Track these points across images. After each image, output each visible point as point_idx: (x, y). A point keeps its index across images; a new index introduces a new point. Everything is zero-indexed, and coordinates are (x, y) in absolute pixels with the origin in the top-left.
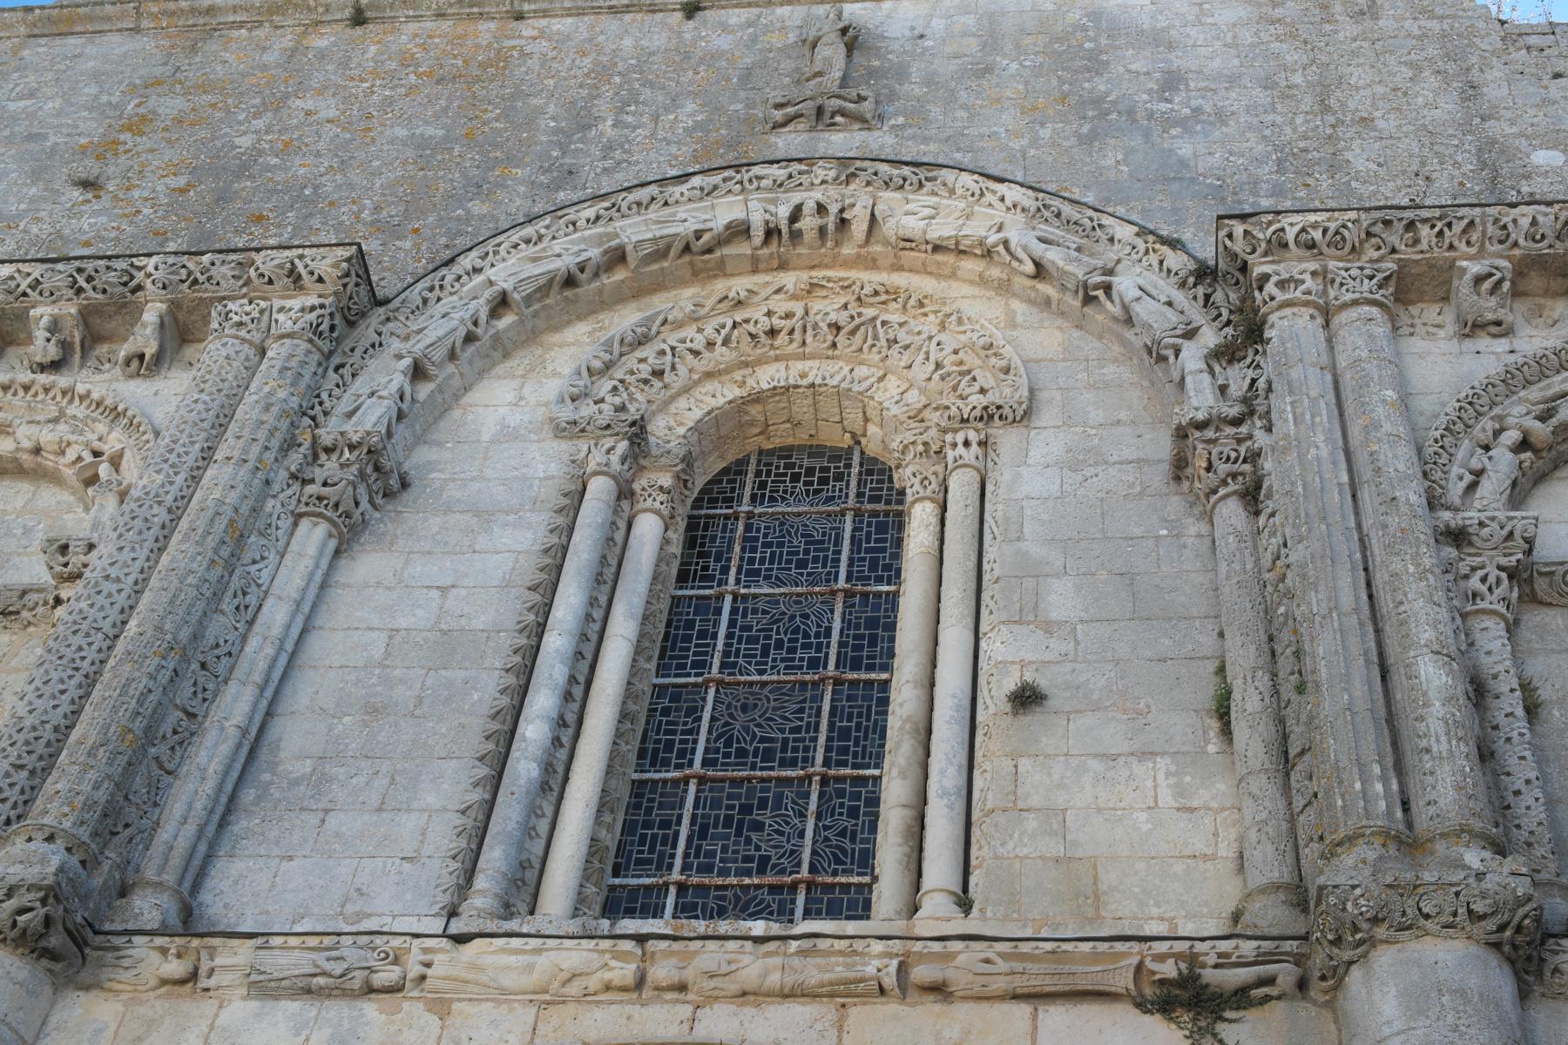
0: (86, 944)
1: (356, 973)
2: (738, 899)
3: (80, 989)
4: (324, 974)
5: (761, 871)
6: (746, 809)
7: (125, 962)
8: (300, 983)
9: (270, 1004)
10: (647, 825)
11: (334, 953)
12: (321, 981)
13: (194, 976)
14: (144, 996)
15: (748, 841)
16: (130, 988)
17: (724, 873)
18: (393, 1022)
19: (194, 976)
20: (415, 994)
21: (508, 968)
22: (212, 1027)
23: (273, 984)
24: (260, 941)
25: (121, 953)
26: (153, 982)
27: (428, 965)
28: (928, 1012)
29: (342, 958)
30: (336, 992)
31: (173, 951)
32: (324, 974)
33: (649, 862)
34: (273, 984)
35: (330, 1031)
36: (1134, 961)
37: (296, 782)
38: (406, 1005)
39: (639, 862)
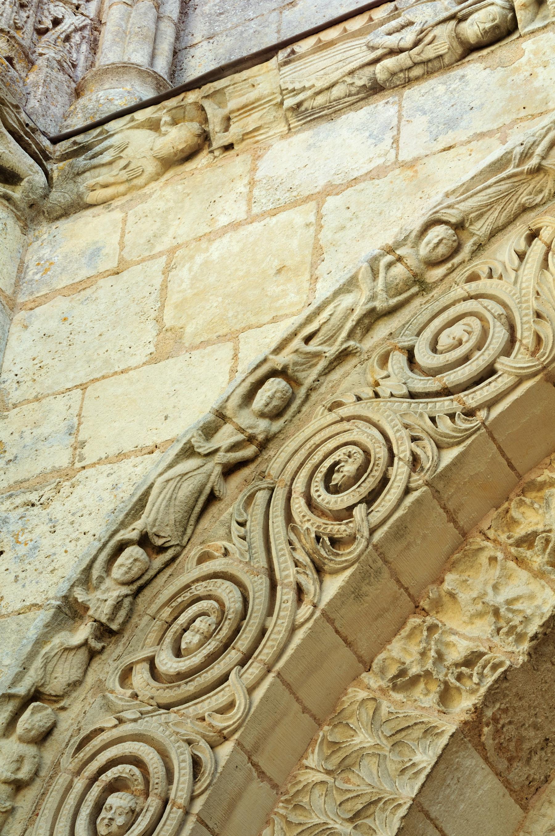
0: (47, 158)
1: (437, 31)
3: (57, 218)
4: (393, 52)
7: (106, 158)
8: (362, 79)
9: (324, 127)
11: (394, 24)
12: (390, 63)
14: (146, 190)
16: (122, 188)
18: (517, 69)
20: (538, 24)
22: (252, 183)
23: (320, 100)
24: (282, 55)
25: (97, 149)
26: (151, 167)
29: (411, 23)
30: (417, 72)
31: (166, 118)
32: (393, 52)
34: (320, 100)
35: (425, 119)
38: (528, 45)
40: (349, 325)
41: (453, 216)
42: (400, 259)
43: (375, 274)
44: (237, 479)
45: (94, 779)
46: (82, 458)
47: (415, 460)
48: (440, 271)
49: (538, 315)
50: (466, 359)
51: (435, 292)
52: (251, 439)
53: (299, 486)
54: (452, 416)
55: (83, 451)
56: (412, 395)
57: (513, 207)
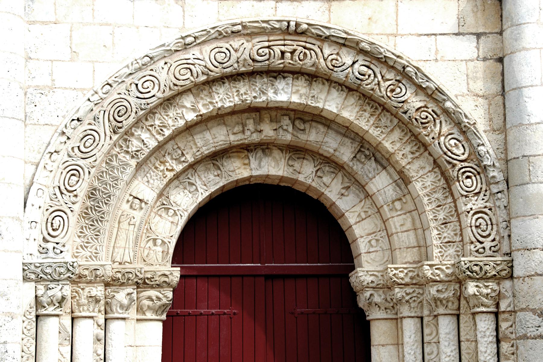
40: (125, 76)
41: (151, 56)
42: (138, 63)
43: (132, 64)
44: (97, 106)
45: (68, 172)
46: (54, 85)
47: (136, 112)
48: (145, 67)
49: (165, 86)
50: (149, 92)
51: (143, 71)
52: (101, 99)
53: (112, 113)
54: (145, 104)
55: (55, 82)
56: (137, 97)
57: (163, 56)
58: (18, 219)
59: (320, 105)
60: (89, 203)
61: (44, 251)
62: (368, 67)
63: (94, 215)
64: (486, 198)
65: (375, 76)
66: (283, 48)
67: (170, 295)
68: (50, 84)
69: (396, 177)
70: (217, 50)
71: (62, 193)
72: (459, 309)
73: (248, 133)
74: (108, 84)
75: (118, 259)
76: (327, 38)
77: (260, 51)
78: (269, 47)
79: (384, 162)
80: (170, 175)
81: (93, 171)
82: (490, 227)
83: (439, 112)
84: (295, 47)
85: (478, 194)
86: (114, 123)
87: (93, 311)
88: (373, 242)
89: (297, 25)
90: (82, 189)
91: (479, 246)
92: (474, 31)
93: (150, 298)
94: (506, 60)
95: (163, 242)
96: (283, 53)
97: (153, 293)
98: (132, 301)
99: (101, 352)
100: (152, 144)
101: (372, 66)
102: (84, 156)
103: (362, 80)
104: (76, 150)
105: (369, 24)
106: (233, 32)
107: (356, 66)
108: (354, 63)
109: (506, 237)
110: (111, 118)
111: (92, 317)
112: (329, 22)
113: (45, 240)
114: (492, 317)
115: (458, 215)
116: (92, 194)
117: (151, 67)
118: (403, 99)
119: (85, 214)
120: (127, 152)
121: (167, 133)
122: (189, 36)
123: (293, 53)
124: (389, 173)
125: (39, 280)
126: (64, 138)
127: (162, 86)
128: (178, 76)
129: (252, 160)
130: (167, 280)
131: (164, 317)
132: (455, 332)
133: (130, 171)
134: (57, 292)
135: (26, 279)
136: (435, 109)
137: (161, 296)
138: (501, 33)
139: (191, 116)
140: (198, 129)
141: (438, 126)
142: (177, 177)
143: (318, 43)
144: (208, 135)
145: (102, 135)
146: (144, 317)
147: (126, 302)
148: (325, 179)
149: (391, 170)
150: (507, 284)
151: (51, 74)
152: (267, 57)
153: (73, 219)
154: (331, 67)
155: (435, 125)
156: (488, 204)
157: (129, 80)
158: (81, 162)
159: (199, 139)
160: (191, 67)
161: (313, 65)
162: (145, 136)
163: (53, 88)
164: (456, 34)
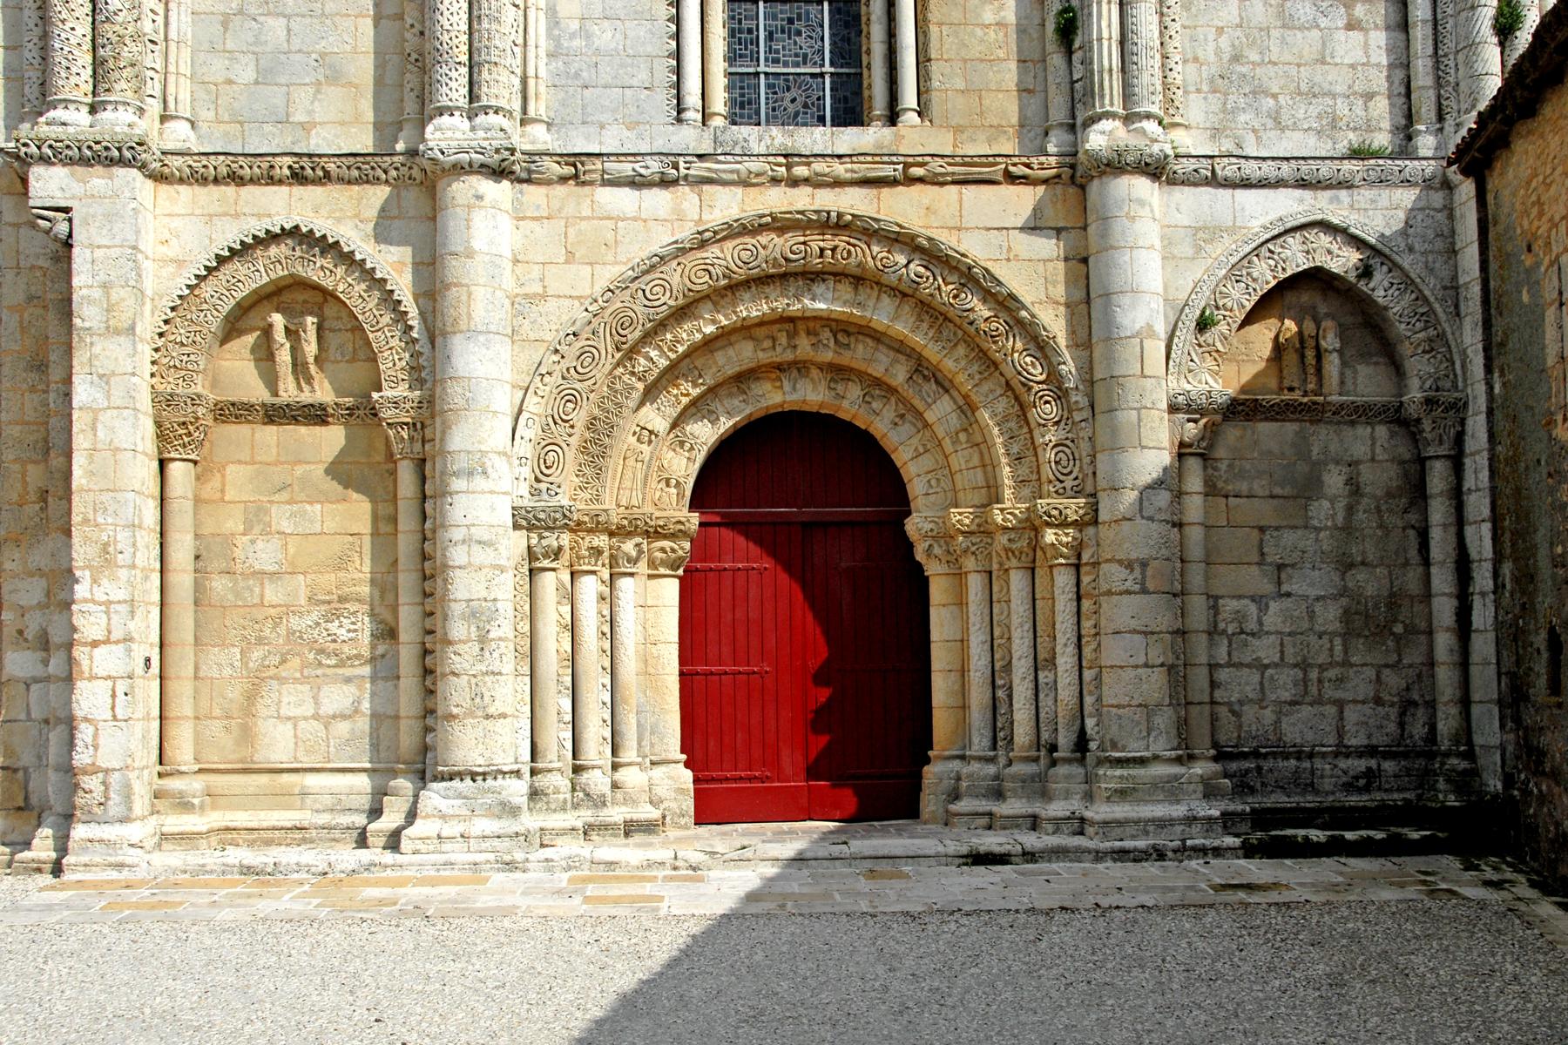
2: (795, 81)
5: (805, 63)
6: (791, 21)
10: (740, 31)
13: (576, 176)
15: (795, 43)
17: (786, 64)
19: (576, 176)
21: (724, 171)
27: (688, 169)
28: (917, 189)
32: (641, 175)
33: (746, 56)
36: (1003, 166)
37: (572, 36)
39: (741, 56)
58: (505, 454)
59: (868, 314)
60: (588, 435)
61: (535, 493)
62: (926, 268)
63: (594, 449)
64: (1068, 428)
65: (935, 279)
66: (821, 244)
67: (687, 545)
68: (540, 291)
69: (961, 402)
70: (741, 247)
71: (555, 423)
72: (1034, 561)
73: (779, 349)
74: (609, 290)
75: (624, 503)
76: (876, 231)
77: (794, 248)
78: (804, 243)
79: (947, 384)
80: (685, 400)
81: (592, 396)
82: (1071, 463)
83: (1011, 323)
84: (837, 243)
85: (1059, 421)
86: (617, 337)
87: (596, 565)
88: (933, 482)
89: (840, 215)
90: (580, 418)
91: (1059, 485)
92: (1053, 225)
93: (663, 550)
94: (1091, 260)
95: (678, 484)
96: (822, 250)
97: (666, 544)
98: (640, 552)
99: (607, 612)
100: (663, 363)
101: (931, 266)
102: (580, 377)
103: (918, 284)
104: (572, 371)
105: (927, 215)
106: (760, 225)
107: (912, 266)
108: (909, 262)
109: (1090, 475)
110: (614, 331)
111: (594, 572)
112: (878, 212)
113: (537, 480)
114: (1072, 570)
115: (1035, 449)
116: (591, 425)
117: (662, 269)
118: (968, 306)
119: (583, 450)
120: (633, 373)
121: (681, 349)
122: (708, 230)
123: (834, 250)
124: (952, 397)
125: (530, 528)
126: (556, 358)
127: (675, 291)
128: (694, 279)
129: (786, 383)
130: (682, 527)
131: (680, 572)
132: (1029, 589)
133: (636, 395)
134: (551, 540)
135: (516, 527)
136: (1008, 319)
137: (676, 547)
138: (1085, 228)
139: (709, 329)
140: (719, 344)
141: (1011, 342)
142: (694, 403)
143: (865, 238)
144: (731, 352)
145: (603, 352)
146: (655, 572)
147: (634, 554)
148: (875, 405)
149: (955, 393)
150: (1091, 530)
151: (542, 280)
152: (803, 255)
153: (570, 454)
154: (881, 267)
155: (1007, 339)
156: (1070, 435)
157: (634, 286)
158: (578, 386)
159: (720, 357)
160: (710, 268)
161: (858, 266)
162: (654, 354)
163: (544, 297)
164: (1032, 229)
